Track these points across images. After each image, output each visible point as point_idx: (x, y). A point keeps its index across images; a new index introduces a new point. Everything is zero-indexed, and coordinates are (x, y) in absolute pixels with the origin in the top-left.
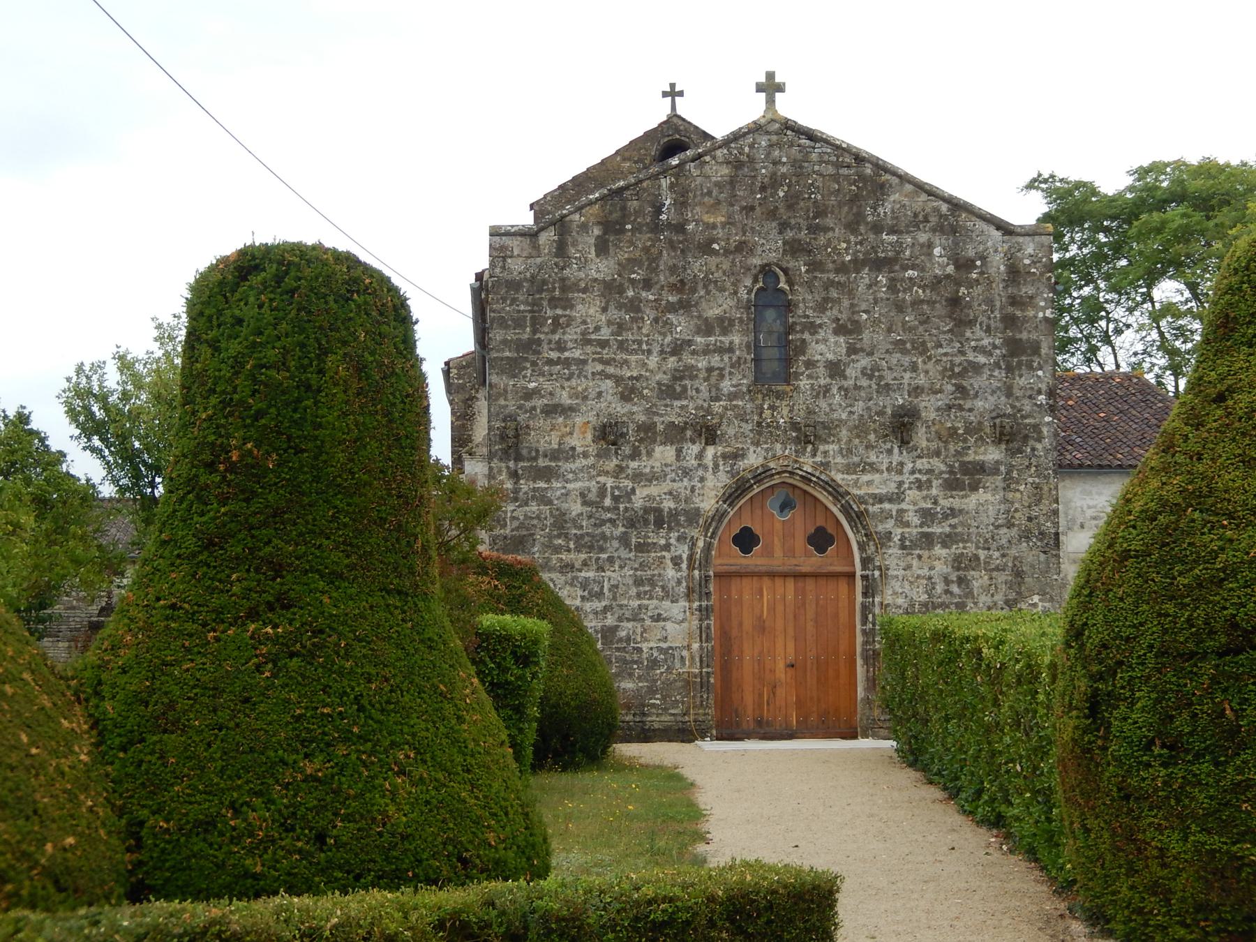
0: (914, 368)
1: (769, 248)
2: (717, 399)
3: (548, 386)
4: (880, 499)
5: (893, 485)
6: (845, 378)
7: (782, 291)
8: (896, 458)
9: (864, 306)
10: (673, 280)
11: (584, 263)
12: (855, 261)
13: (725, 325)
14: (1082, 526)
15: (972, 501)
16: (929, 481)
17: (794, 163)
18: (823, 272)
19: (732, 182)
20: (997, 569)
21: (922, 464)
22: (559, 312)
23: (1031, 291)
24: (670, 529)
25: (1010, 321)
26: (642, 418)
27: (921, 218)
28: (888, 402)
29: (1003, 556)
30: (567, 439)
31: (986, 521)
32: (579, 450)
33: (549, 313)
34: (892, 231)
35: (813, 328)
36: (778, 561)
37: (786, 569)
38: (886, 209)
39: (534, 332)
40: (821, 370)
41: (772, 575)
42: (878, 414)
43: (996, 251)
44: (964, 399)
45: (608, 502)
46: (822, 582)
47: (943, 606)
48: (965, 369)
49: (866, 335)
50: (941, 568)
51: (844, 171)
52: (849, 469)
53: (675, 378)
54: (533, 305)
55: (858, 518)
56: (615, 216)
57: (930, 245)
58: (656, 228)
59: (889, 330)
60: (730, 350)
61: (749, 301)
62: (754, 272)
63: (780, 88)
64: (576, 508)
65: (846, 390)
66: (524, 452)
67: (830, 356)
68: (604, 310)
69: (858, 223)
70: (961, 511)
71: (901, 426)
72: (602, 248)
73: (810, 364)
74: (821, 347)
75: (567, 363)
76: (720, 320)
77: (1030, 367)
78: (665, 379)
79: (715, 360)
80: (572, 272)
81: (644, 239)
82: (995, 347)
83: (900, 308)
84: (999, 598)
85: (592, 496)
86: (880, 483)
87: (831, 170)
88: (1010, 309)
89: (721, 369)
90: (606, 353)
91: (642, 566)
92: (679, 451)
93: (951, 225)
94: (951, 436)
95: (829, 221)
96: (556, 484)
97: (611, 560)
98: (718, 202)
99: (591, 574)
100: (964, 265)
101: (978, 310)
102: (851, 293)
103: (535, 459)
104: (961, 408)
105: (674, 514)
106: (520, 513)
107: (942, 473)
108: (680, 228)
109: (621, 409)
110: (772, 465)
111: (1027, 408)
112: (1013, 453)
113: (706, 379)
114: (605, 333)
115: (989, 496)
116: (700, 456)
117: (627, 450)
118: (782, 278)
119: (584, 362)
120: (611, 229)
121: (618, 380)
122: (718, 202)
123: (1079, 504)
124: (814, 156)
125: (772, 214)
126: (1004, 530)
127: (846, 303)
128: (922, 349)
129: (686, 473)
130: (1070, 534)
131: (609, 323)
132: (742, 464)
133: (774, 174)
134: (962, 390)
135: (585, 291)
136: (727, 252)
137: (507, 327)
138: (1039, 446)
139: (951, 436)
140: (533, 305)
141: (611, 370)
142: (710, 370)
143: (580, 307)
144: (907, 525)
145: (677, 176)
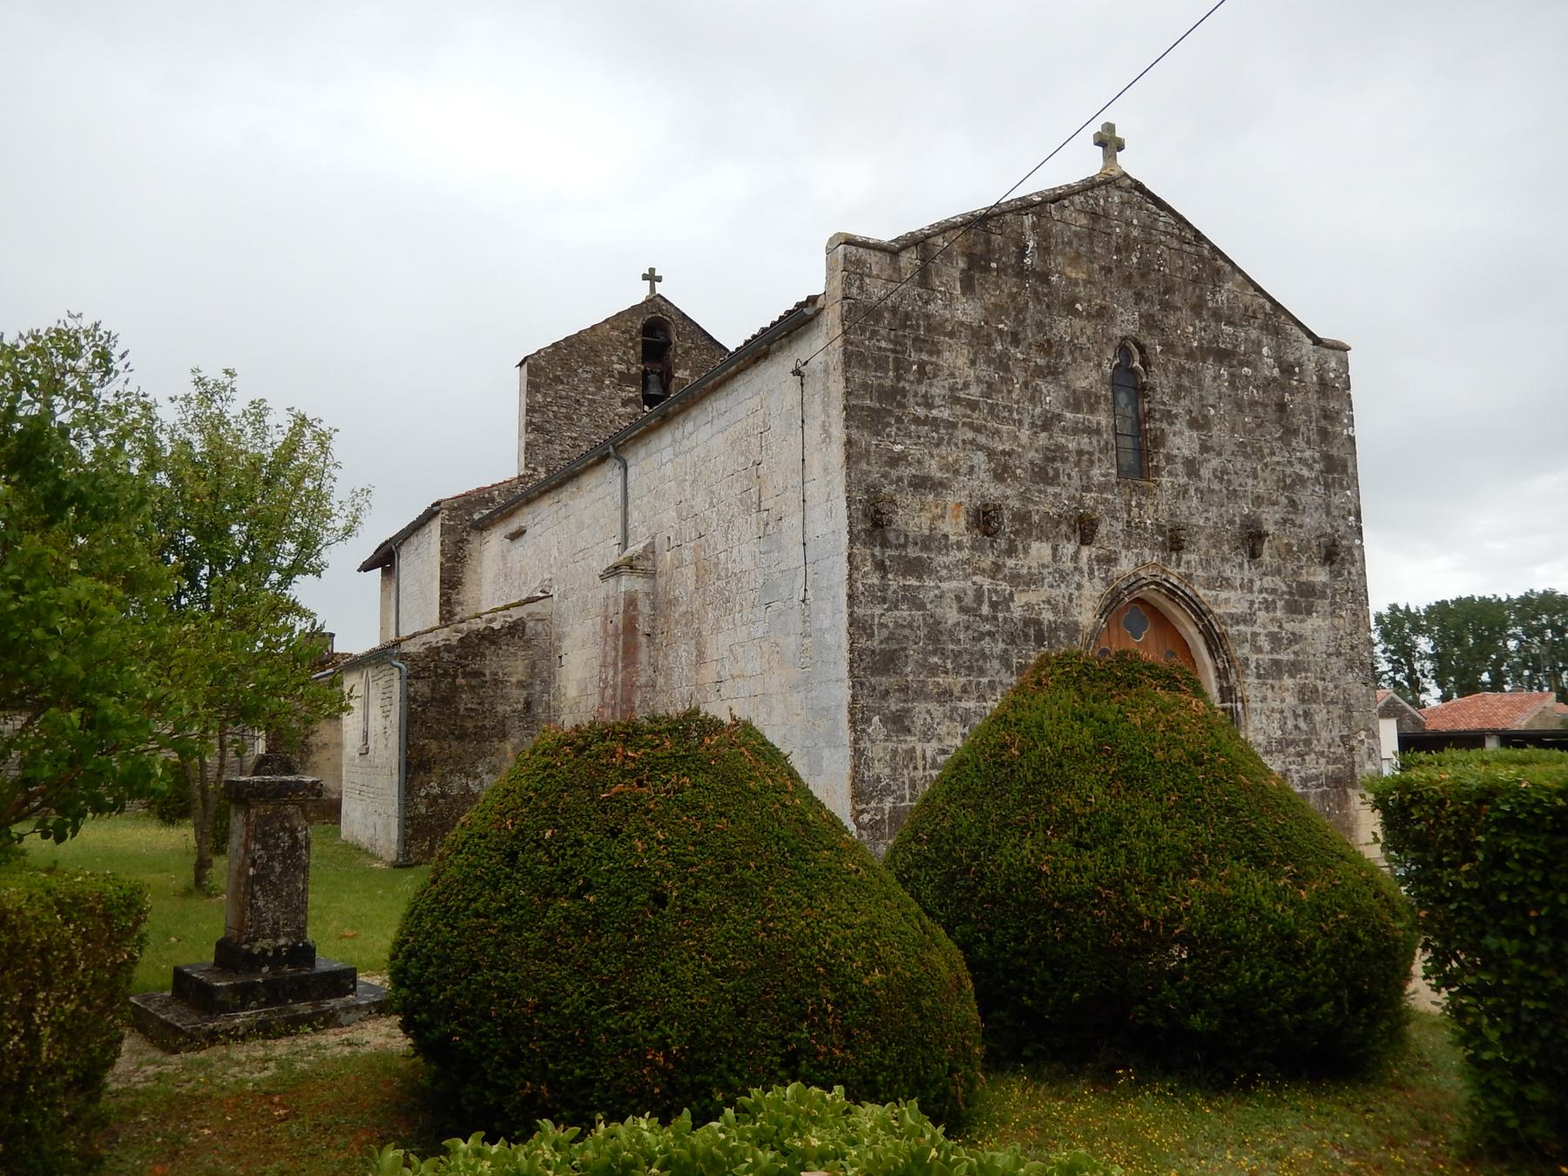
1: (1127, 322)
3: (915, 452)
5: (1247, 605)
7: (1134, 371)
9: (1211, 401)
10: (1040, 337)
11: (950, 302)
12: (1200, 347)
16: (1274, 602)
18: (1175, 355)
19: (1091, 235)
20: (1332, 702)
21: (1268, 582)
26: (1015, 504)
27: (1250, 313)
30: (939, 523)
33: (914, 357)
34: (1228, 323)
35: (1170, 417)
38: (1222, 297)
39: (899, 378)
40: (1180, 468)
47: (1293, 743)
48: (1294, 483)
49: (1215, 431)
50: (1291, 700)
51: (1186, 247)
52: (1209, 584)
54: (896, 343)
55: (1215, 642)
56: (979, 249)
57: (1259, 344)
58: (1021, 273)
63: (659, 279)
64: (952, 616)
66: (891, 536)
67: (1186, 452)
68: (973, 363)
71: (1252, 539)
72: (968, 287)
73: (1170, 459)
74: (1178, 440)
75: (935, 423)
76: (1087, 393)
78: (1037, 457)
80: (935, 308)
81: (1009, 284)
83: (1239, 406)
85: (969, 601)
92: (1055, 549)
95: (1177, 299)
96: (929, 583)
99: (971, 705)
100: (1287, 369)
103: (904, 546)
106: (888, 619)
107: (1283, 593)
108: (1044, 277)
109: (994, 491)
113: (1077, 464)
114: (975, 392)
116: (1075, 557)
118: (1137, 357)
119: (954, 425)
120: (977, 265)
121: (991, 454)
127: (1197, 394)
131: (979, 380)
132: (1116, 571)
134: (1292, 503)
135: (951, 335)
136: (1089, 317)
137: (866, 367)
144: (1259, 650)
145: (1039, 215)
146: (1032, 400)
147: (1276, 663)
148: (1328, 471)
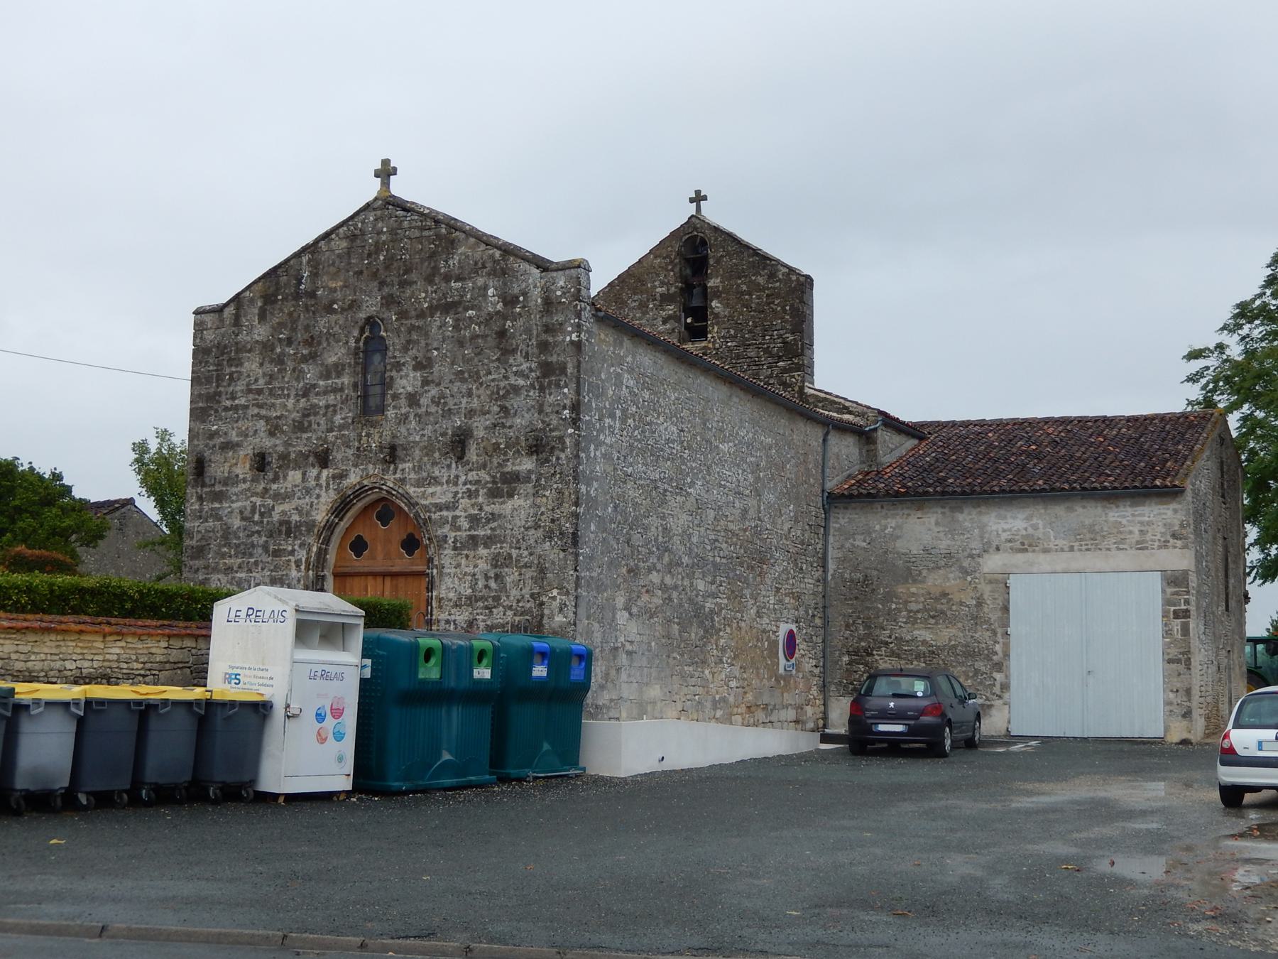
0: (470, 394)
1: (371, 305)
2: (331, 430)
4: (439, 507)
5: (451, 495)
6: (419, 406)
7: (382, 338)
8: (453, 472)
9: (435, 345)
12: (430, 307)
13: (338, 369)
14: (998, 549)
15: (509, 505)
16: (477, 490)
17: (392, 232)
18: (407, 319)
20: (525, 566)
21: (473, 476)
22: (233, 369)
23: (560, 318)
24: (295, 538)
25: (544, 347)
26: (281, 449)
27: (480, 265)
28: (450, 424)
29: (531, 554)
30: (234, 469)
31: (519, 524)
32: (241, 477)
35: (398, 366)
36: (380, 565)
37: (366, 570)
38: (454, 261)
40: (403, 402)
41: (375, 575)
42: (442, 435)
43: (535, 287)
44: (506, 417)
45: (257, 517)
46: (410, 579)
47: (482, 598)
48: (508, 392)
49: (436, 368)
50: (483, 566)
51: (426, 233)
52: (419, 484)
53: (305, 416)
54: (218, 365)
57: (486, 288)
59: (453, 363)
60: (342, 390)
61: (357, 348)
62: (360, 323)
64: (236, 523)
65: (420, 416)
66: (207, 480)
67: (410, 389)
68: (261, 365)
69: (434, 275)
70: (500, 515)
71: (459, 444)
72: (262, 317)
73: (395, 397)
74: (404, 382)
76: (336, 365)
77: (558, 386)
78: (295, 415)
79: (331, 399)
81: (289, 307)
82: (531, 370)
83: (461, 343)
84: (526, 591)
85: (247, 513)
86: (440, 494)
87: (417, 233)
88: (544, 337)
89: (335, 406)
90: (261, 399)
91: (276, 568)
92: (304, 474)
93: (502, 269)
94: (495, 450)
97: (256, 563)
98: (339, 270)
99: (243, 575)
100: (510, 301)
101: (519, 340)
102: (427, 335)
104: (503, 426)
105: (298, 525)
106: (202, 529)
107: (487, 482)
108: (312, 294)
109: (268, 443)
110: (365, 482)
111: (555, 422)
112: (541, 463)
113: (325, 415)
115: (521, 502)
116: (318, 478)
117: (270, 475)
121: (268, 419)
122: (339, 270)
123: (994, 528)
124: (406, 224)
125: (375, 275)
126: (532, 532)
127: (423, 343)
128: (476, 377)
129: (308, 491)
130: (986, 556)
131: (264, 375)
132: (346, 483)
133: (377, 243)
134: (504, 409)
135: (250, 351)
138: (563, 456)
139: (495, 450)
140: (218, 365)
141: (263, 412)
142: (327, 407)
143: (246, 364)
144: (459, 529)
146: (298, 379)
147: (473, 538)
148: (545, 376)
